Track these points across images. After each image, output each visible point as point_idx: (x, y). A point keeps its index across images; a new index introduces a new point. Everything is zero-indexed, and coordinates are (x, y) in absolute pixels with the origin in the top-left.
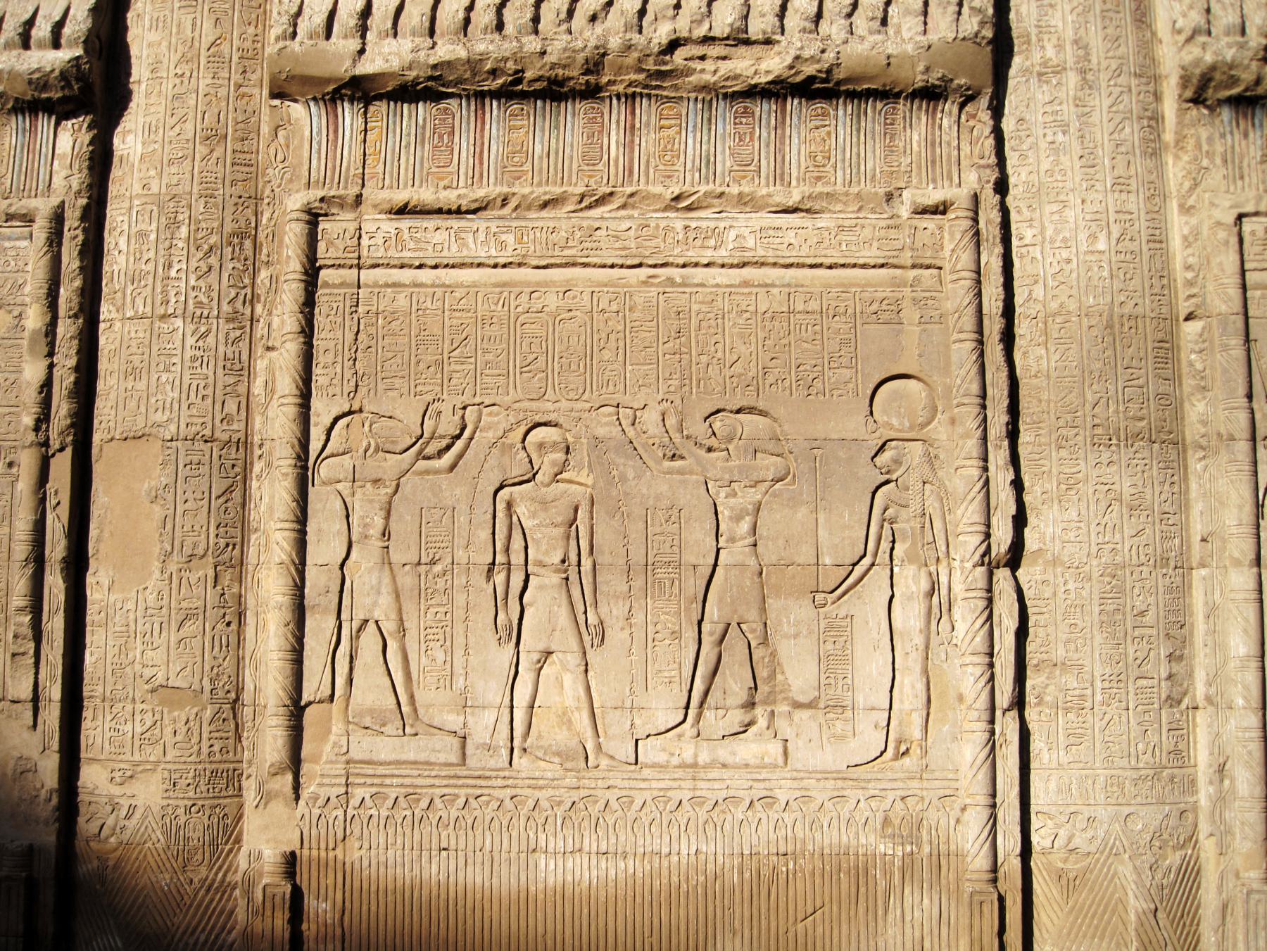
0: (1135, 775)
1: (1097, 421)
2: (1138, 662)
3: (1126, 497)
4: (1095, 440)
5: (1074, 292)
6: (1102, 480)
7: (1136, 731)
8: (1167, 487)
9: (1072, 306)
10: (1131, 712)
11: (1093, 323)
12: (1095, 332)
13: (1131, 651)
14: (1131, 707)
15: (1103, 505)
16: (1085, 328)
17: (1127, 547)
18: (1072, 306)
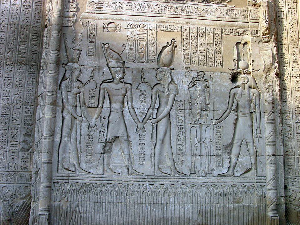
0: (7, 173)
1: (8, 57)
2: (12, 136)
3: (15, 82)
4: (7, 64)
5: (7, 17)
6: (7, 76)
7: (9, 159)
8: (31, 79)
9: (6, 21)
10: (8, 152)
11: (12, 27)
12: (12, 29)
13: (10, 132)
14: (8, 150)
15: (6, 85)
16: (9, 29)
17: (13, 98)
18: (6, 21)
